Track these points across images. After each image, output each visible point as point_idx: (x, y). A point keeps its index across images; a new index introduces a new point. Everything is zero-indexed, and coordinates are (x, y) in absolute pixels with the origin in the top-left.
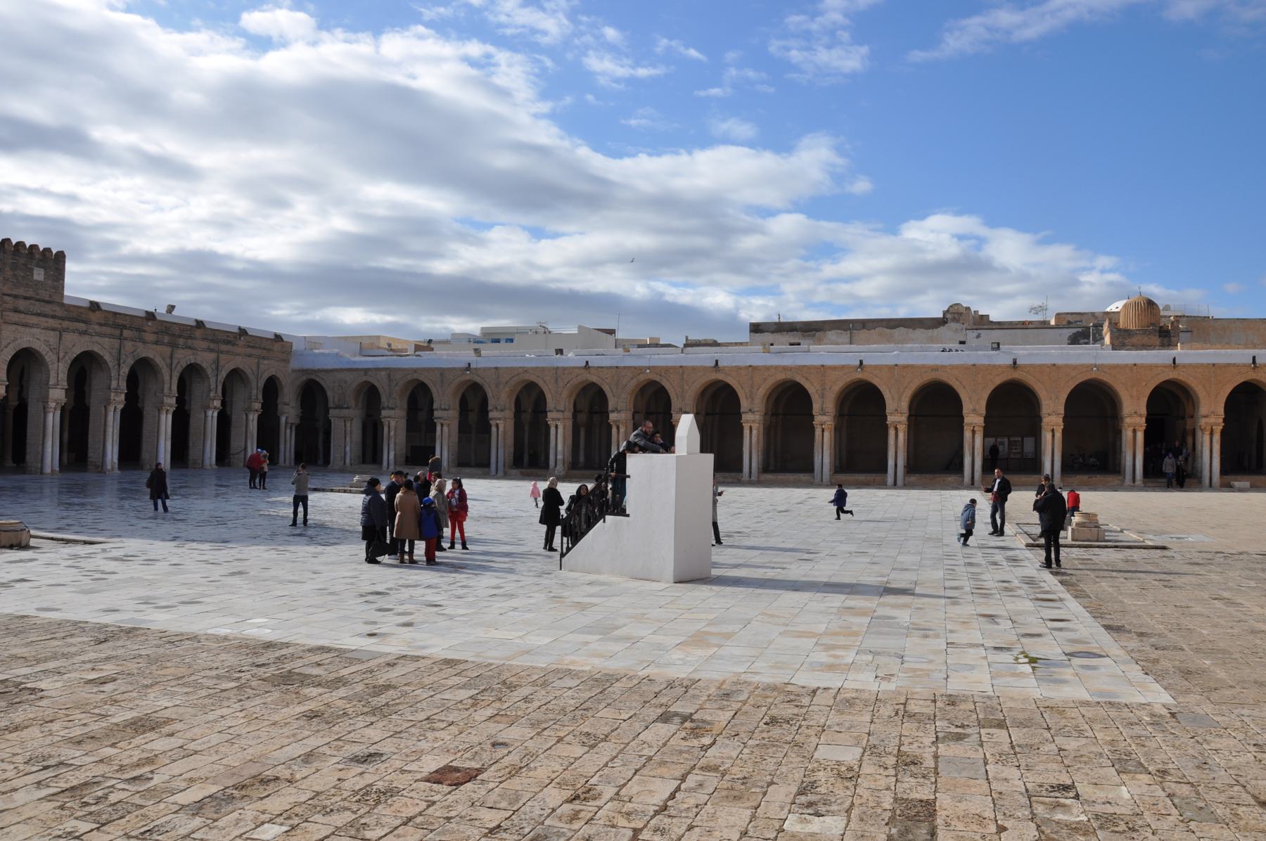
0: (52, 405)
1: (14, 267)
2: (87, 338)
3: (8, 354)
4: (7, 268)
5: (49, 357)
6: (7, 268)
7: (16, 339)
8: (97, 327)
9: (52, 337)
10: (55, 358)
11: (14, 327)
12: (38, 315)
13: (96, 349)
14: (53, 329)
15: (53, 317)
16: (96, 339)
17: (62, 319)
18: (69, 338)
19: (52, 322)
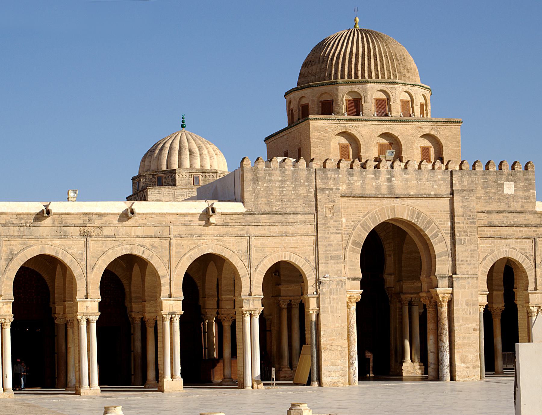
1: (486, 185)
4: (479, 188)
7: (493, 251)
12: (512, 226)
15: (526, 226)
19: (526, 232)
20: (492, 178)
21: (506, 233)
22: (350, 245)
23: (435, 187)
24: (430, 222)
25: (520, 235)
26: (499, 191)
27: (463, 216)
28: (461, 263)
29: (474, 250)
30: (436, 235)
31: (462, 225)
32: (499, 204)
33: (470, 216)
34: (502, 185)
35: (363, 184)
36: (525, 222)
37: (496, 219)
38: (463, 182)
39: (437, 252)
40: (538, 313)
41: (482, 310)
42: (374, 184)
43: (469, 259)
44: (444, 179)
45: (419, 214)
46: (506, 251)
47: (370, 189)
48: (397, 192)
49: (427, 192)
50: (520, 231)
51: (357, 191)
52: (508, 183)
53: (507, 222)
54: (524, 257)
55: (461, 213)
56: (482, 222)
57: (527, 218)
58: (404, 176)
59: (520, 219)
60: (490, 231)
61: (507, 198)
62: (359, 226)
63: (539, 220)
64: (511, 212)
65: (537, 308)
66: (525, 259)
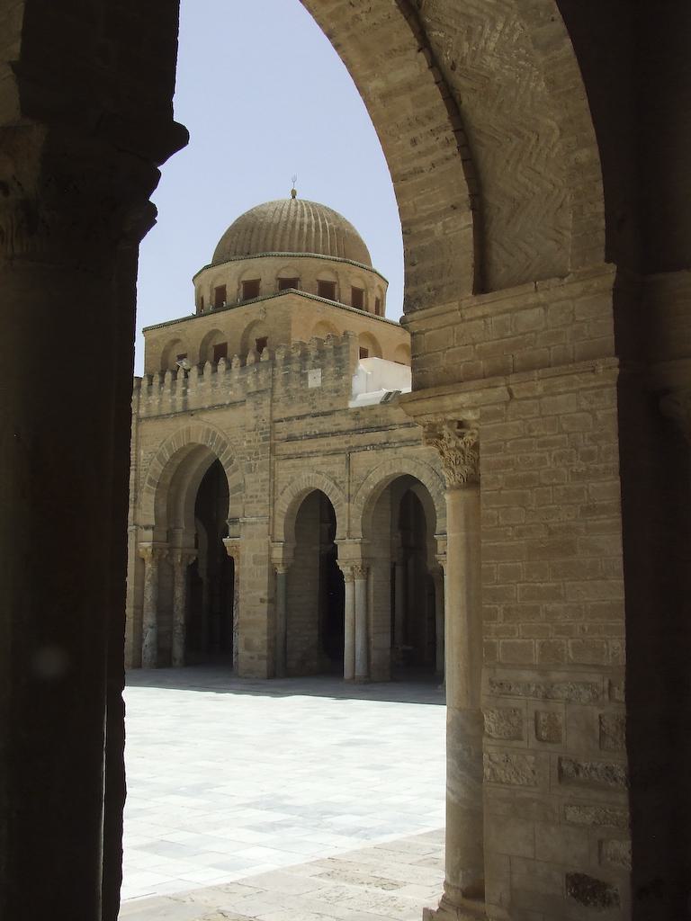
0: (346, 570)
2: (388, 452)
3: (285, 503)
5: (335, 497)
6: (278, 385)
8: (404, 433)
9: (337, 466)
10: (341, 495)
11: (292, 461)
13: (407, 468)
14: (336, 452)
15: (333, 434)
16: (404, 450)
17: (346, 432)
18: (362, 459)
19: (335, 442)
20: (295, 367)
21: (309, 450)
22: (146, 484)
23: (230, 393)
24: (224, 445)
25: (328, 448)
26: (302, 385)
27: (255, 430)
28: (250, 500)
29: (265, 480)
30: (231, 462)
31: (253, 444)
32: (301, 405)
33: (263, 429)
34: (304, 376)
35: (160, 403)
36: (334, 429)
37: (297, 428)
38: (258, 380)
39: (231, 485)
40: (353, 577)
41: (280, 570)
42: (170, 401)
43: (259, 494)
44: (239, 381)
45: (214, 434)
46: (309, 478)
47: (166, 409)
48: (191, 407)
49: (220, 402)
50: (328, 445)
51: (155, 412)
52: (314, 370)
53: (311, 432)
54: (332, 484)
55: (252, 428)
56: (280, 436)
57: (336, 422)
58: (199, 385)
59: (327, 424)
60: (289, 448)
61: (311, 395)
62: (155, 458)
63: (353, 423)
64: (316, 415)
65: (349, 568)
66: (333, 489)
